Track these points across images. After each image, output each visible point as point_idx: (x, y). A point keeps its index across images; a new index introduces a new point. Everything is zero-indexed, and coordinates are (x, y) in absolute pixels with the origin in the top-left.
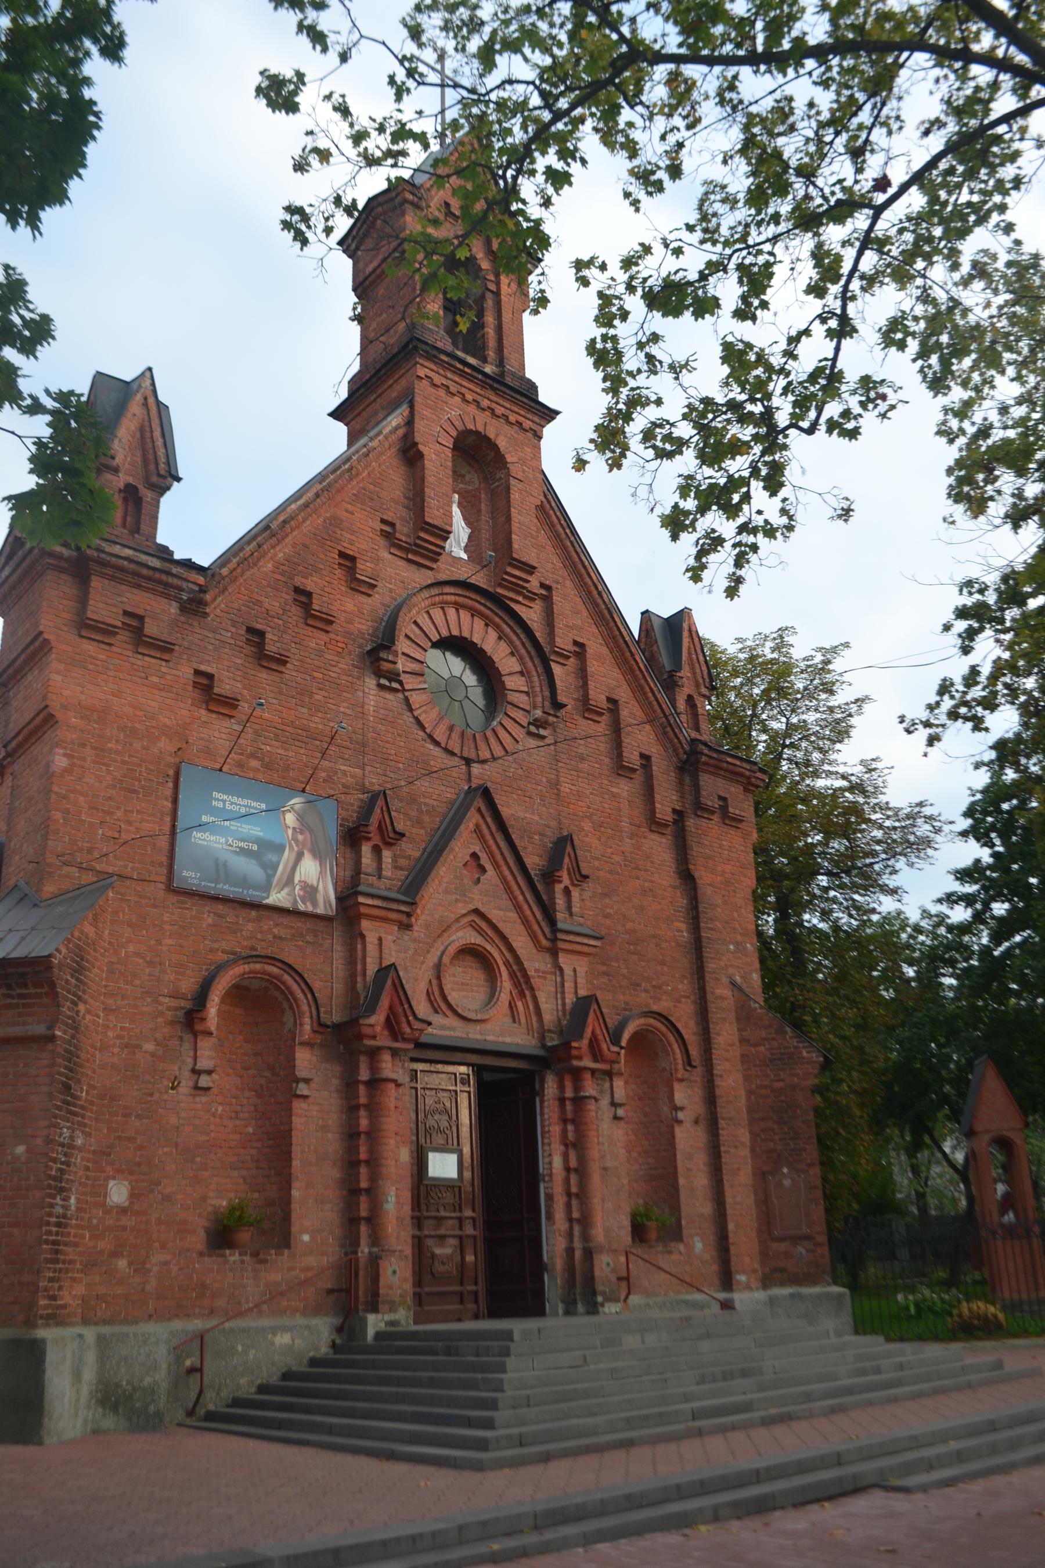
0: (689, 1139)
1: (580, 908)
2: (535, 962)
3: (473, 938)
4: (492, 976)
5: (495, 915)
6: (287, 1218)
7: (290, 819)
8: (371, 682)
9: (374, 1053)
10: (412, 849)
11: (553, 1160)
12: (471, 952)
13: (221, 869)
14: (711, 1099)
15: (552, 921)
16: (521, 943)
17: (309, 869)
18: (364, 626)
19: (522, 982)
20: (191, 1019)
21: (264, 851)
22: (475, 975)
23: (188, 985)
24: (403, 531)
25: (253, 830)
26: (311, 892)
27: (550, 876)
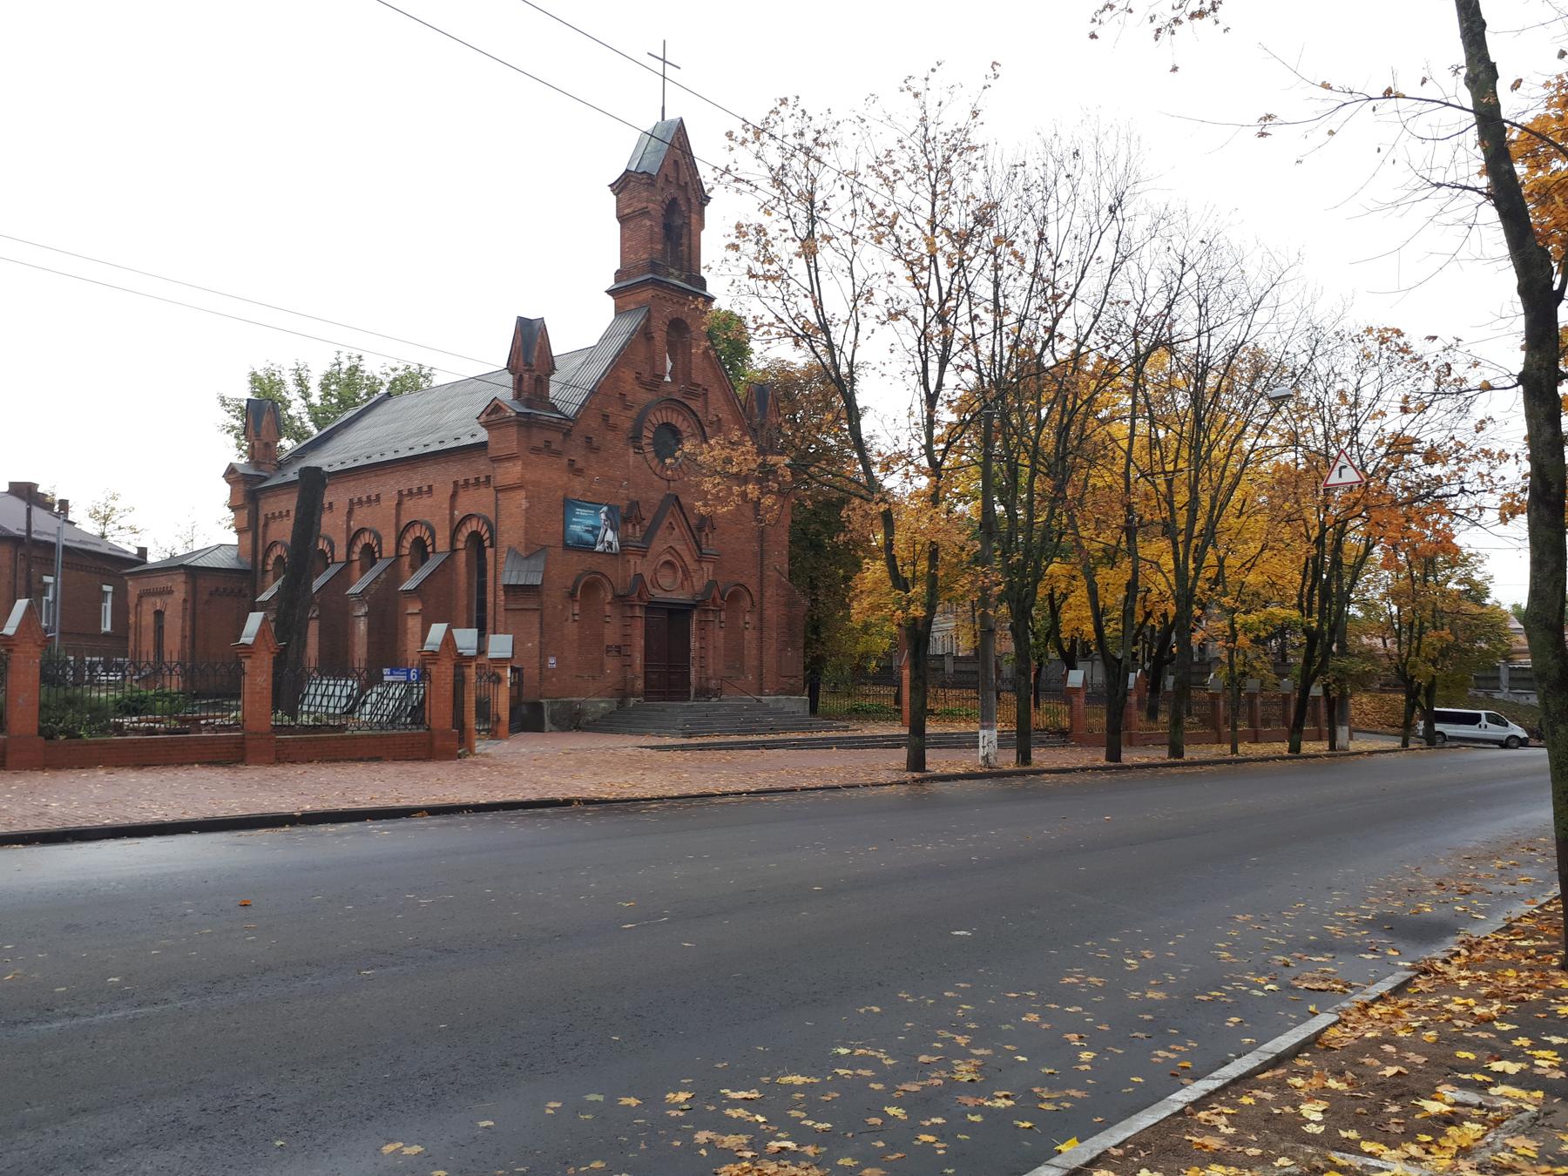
0: (750, 636)
1: (711, 543)
2: (692, 566)
3: (669, 558)
4: (675, 571)
5: (678, 547)
6: (602, 665)
7: (603, 516)
8: (631, 450)
9: (632, 606)
10: (647, 523)
11: (694, 644)
12: (667, 562)
13: (580, 538)
14: (761, 620)
15: (700, 548)
16: (687, 559)
17: (610, 536)
18: (628, 425)
19: (686, 573)
20: (572, 595)
21: (594, 530)
22: (667, 571)
23: (570, 583)
24: (646, 377)
25: (590, 522)
26: (610, 544)
27: (700, 529)
